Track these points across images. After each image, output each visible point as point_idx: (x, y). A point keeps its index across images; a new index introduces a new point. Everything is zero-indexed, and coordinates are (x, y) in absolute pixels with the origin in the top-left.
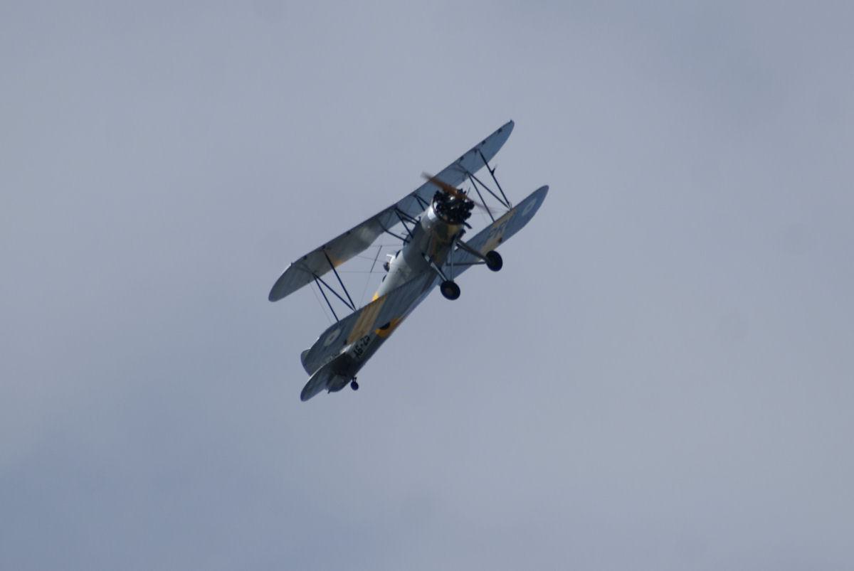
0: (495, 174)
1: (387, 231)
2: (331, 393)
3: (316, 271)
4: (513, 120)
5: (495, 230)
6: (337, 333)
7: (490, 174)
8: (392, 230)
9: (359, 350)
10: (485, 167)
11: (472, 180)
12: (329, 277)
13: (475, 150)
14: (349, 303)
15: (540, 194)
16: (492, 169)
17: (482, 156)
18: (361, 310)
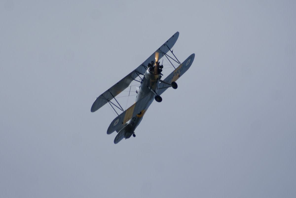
0: (173, 53)
1: (134, 79)
2: (127, 139)
3: (108, 99)
4: (178, 31)
5: (175, 73)
6: (118, 120)
7: (171, 53)
8: (136, 79)
9: (133, 123)
10: (170, 51)
11: (166, 56)
12: (113, 100)
13: (164, 45)
14: (121, 109)
15: (192, 57)
16: (172, 51)
17: (167, 46)
18: (126, 111)
